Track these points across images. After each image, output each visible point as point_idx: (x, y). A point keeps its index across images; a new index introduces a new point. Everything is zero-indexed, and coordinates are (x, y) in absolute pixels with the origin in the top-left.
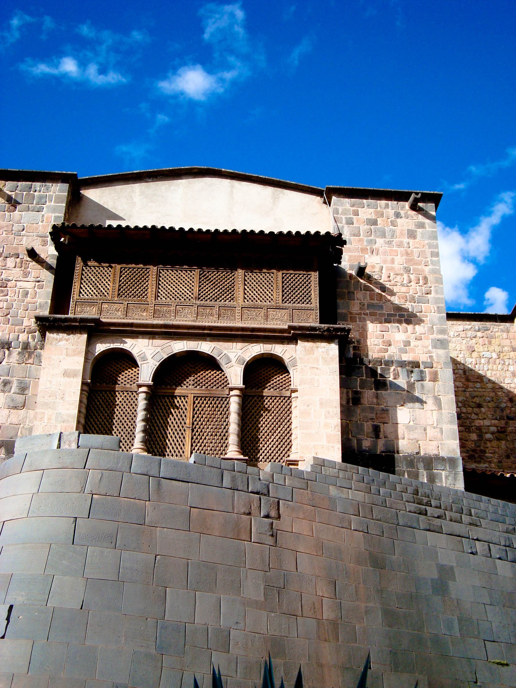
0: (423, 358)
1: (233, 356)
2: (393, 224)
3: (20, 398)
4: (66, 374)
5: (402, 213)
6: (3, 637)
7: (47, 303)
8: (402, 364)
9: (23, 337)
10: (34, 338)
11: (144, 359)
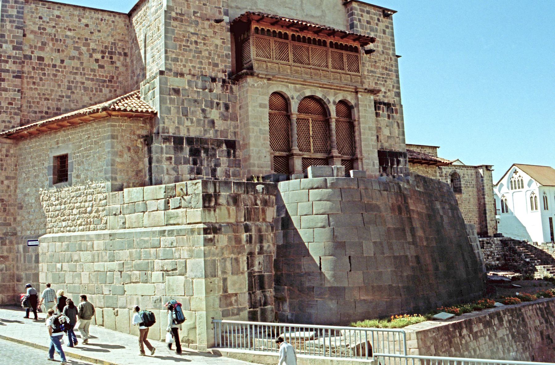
0: (392, 102)
1: (331, 100)
2: (377, 25)
3: (225, 113)
4: (261, 106)
5: (380, 18)
6: (350, 271)
7: (229, 54)
8: (385, 104)
9: (221, 75)
10: (225, 75)
11: (293, 98)
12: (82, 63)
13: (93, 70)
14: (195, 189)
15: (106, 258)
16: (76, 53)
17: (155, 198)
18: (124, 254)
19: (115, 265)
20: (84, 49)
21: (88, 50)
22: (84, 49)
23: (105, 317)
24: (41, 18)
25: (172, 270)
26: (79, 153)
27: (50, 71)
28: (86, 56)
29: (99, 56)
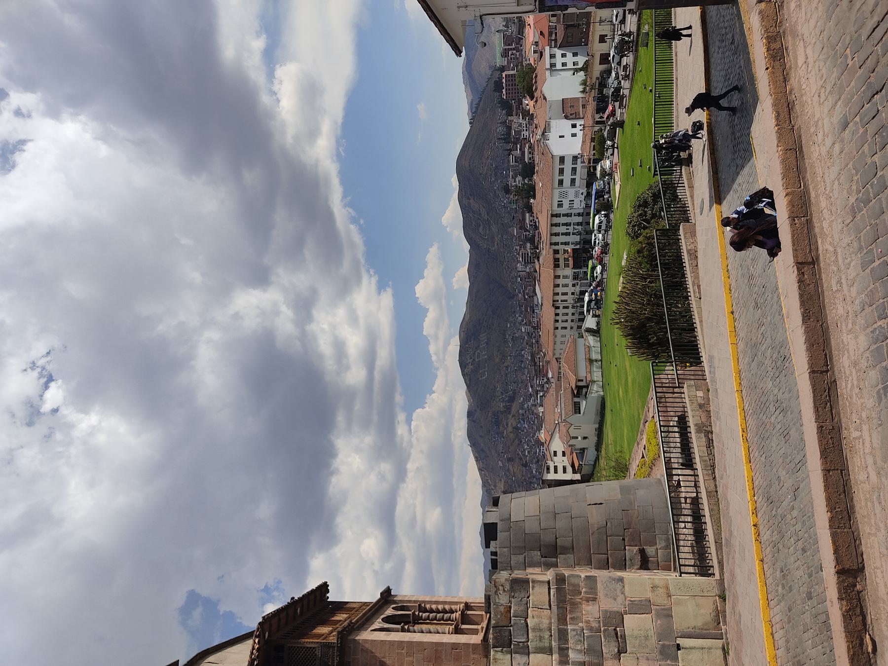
14: (504, 590)
25: (617, 638)
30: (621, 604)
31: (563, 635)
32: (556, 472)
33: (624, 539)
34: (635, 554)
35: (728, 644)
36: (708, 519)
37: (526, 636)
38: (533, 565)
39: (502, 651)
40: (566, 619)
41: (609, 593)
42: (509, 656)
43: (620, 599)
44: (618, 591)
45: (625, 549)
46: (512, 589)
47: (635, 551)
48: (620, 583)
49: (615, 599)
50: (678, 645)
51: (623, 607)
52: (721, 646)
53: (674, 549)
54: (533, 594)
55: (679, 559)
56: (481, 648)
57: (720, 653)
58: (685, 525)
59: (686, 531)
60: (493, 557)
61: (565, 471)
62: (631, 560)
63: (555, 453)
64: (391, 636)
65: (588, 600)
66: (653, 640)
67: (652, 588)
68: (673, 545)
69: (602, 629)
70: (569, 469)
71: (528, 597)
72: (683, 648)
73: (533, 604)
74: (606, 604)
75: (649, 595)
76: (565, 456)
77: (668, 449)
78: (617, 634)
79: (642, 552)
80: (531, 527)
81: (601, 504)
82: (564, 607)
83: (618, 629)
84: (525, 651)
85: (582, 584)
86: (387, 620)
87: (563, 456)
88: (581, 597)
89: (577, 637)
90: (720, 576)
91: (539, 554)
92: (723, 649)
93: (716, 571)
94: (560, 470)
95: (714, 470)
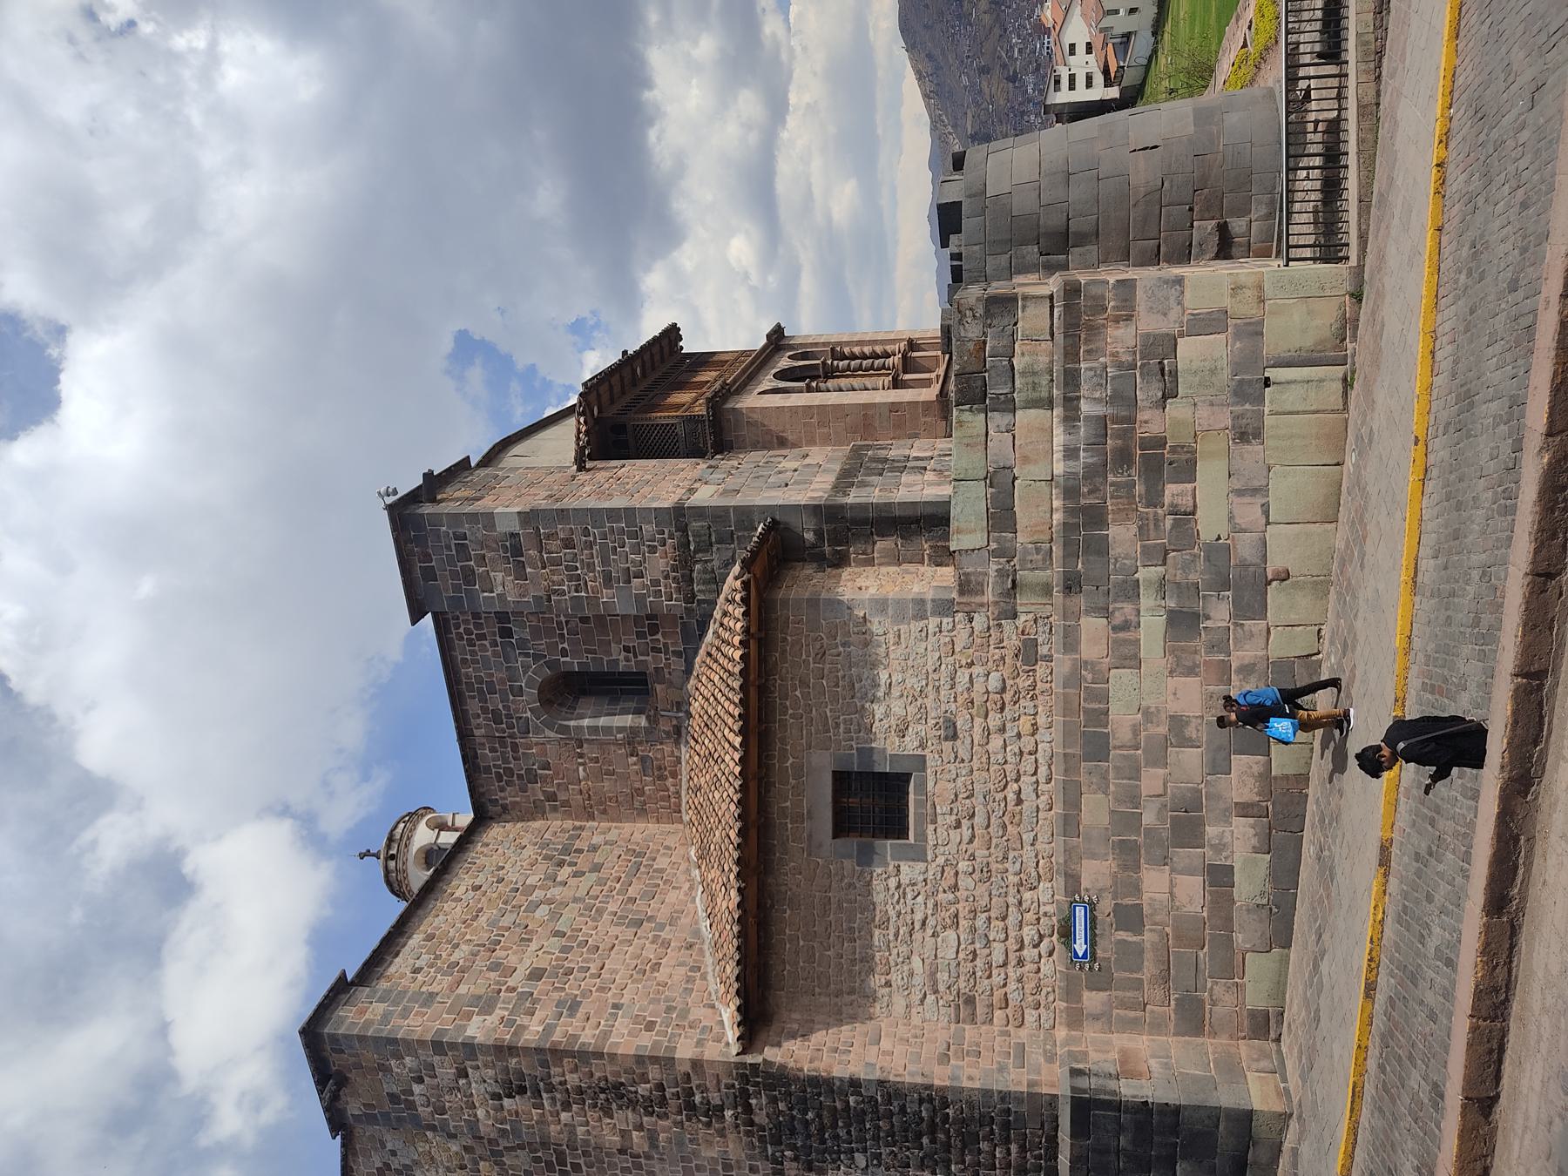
12: (576, 900)
13: (602, 882)
14: (974, 316)
15: (1128, 607)
16: (543, 911)
17: (984, 438)
18: (1121, 535)
19: (1147, 574)
20: (538, 894)
21: (541, 888)
22: (538, 894)
23: (1294, 618)
24: (416, 971)
25: (1163, 375)
26: (838, 725)
27: (574, 960)
28: (555, 892)
29: (565, 872)
30: (1175, 322)
31: (1072, 379)
32: (1072, 87)
33: (1191, 209)
34: (1210, 234)
35: (1353, 372)
36: (1352, 160)
37: (1010, 385)
38: (1025, 269)
39: (971, 410)
40: (1078, 354)
41: (1154, 306)
42: (983, 415)
43: (1174, 314)
44: (1172, 300)
45: (1192, 226)
46: (988, 313)
47: (1210, 227)
48: (1178, 287)
49: (1165, 315)
50: (1267, 379)
51: (1177, 325)
52: (1341, 375)
53: (1281, 218)
54: (1023, 318)
55: (1288, 235)
56: (936, 408)
57: (1339, 386)
58: (1308, 174)
59: (1308, 185)
60: (955, 263)
61: (1089, 84)
62: (1201, 245)
63: (1072, 47)
64: (791, 399)
65: (1117, 320)
66: (1225, 374)
67: (1233, 289)
68: (1281, 211)
69: (1139, 364)
70: (1099, 79)
71: (1016, 324)
72: (1274, 383)
73: (1022, 335)
74: (1148, 322)
75: (1227, 302)
76: (1091, 53)
77: (1296, 25)
78: (1162, 370)
79: (1223, 229)
80: (1023, 203)
81: (1156, 147)
82: (1076, 335)
83: (1166, 362)
84: (1009, 406)
85: (1109, 295)
86: (783, 375)
87: (1087, 53)
88: (1105, 316)
89: (1095, 379)
90: (1359, 260)
91: (1036, 250)
92: (1345, 380)
93: (1353, 253)
94: (1081, 81)
95: (1380, 61)
